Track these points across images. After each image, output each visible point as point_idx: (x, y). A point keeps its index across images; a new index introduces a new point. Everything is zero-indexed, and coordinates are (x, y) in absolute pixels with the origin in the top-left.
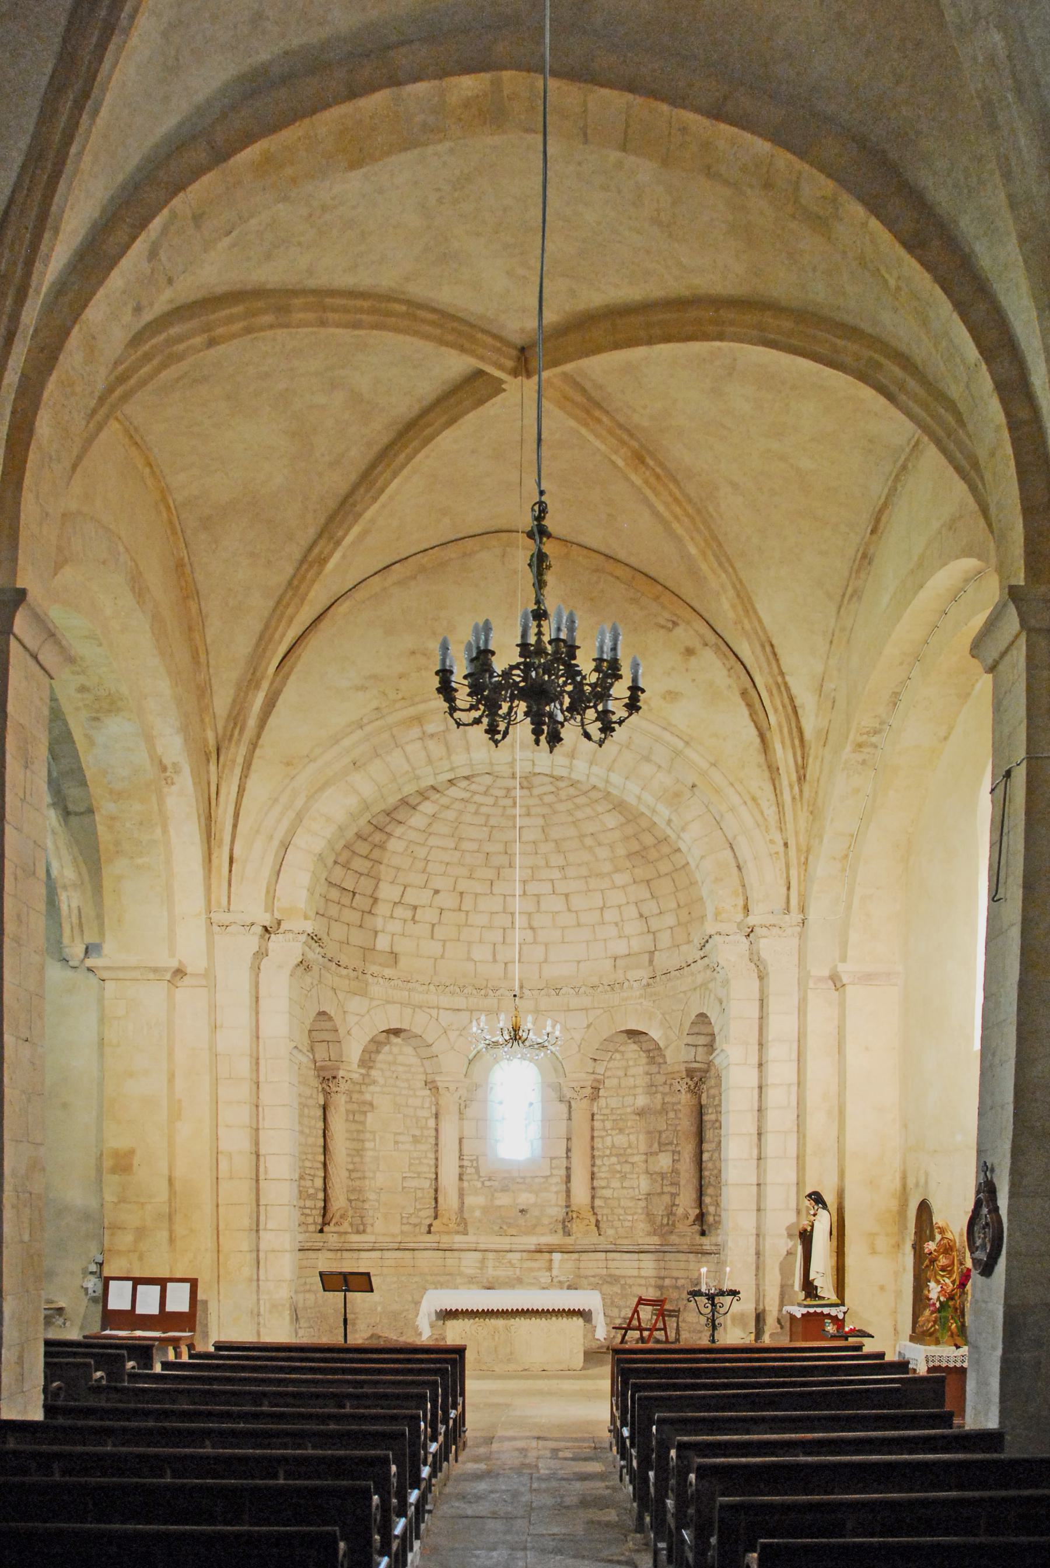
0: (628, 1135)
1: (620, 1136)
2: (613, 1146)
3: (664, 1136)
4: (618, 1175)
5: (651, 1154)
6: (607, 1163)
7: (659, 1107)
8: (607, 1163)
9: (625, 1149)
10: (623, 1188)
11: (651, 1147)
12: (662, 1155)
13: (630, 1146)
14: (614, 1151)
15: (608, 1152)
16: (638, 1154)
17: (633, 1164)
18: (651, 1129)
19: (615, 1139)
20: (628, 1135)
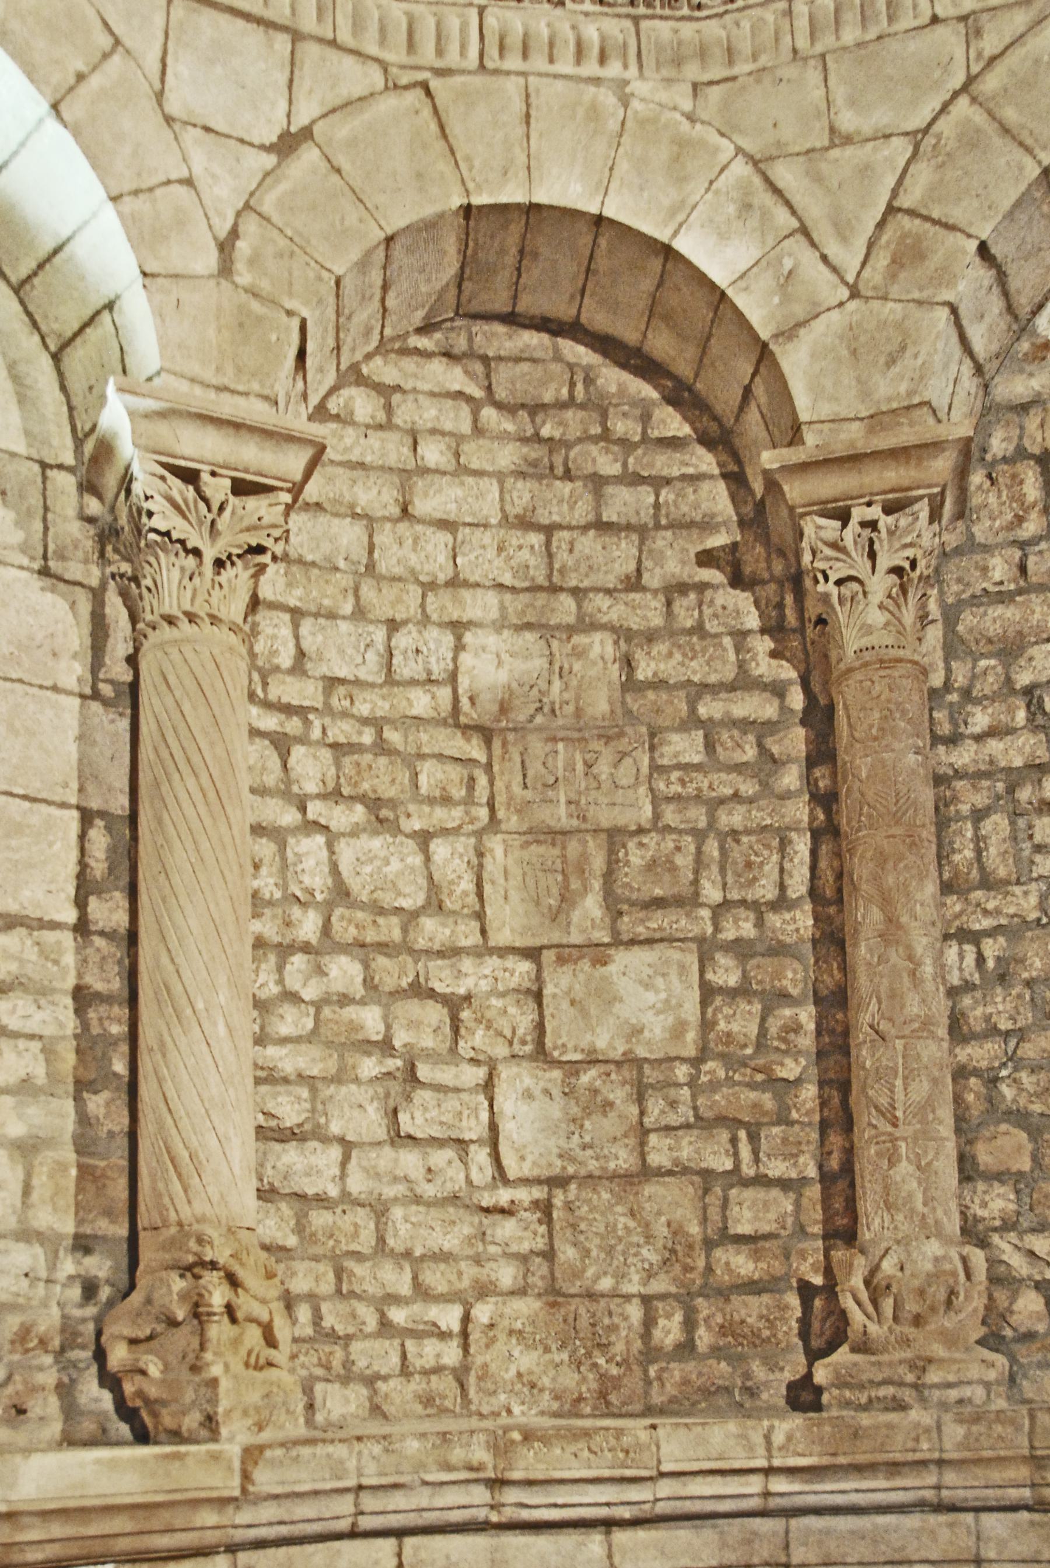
0: (424, 839)
1: (376, 844)
2: (341, 892)
3: (635, 856)
4: (369, 1066)
5: (566, 954)
6: (309, 993)
7: (599, 704)
8: (309, 993)
9: (410, 918)
10: (399, 1138)
11: (557, 916)
12: (639, 958)
13: (435, 904)
14: (344, 930)
15: (308, 927)
16: (485, 950)
17: (454, 1004)
18: (560, 816)
19: (347, 853)
20: (424, 839)
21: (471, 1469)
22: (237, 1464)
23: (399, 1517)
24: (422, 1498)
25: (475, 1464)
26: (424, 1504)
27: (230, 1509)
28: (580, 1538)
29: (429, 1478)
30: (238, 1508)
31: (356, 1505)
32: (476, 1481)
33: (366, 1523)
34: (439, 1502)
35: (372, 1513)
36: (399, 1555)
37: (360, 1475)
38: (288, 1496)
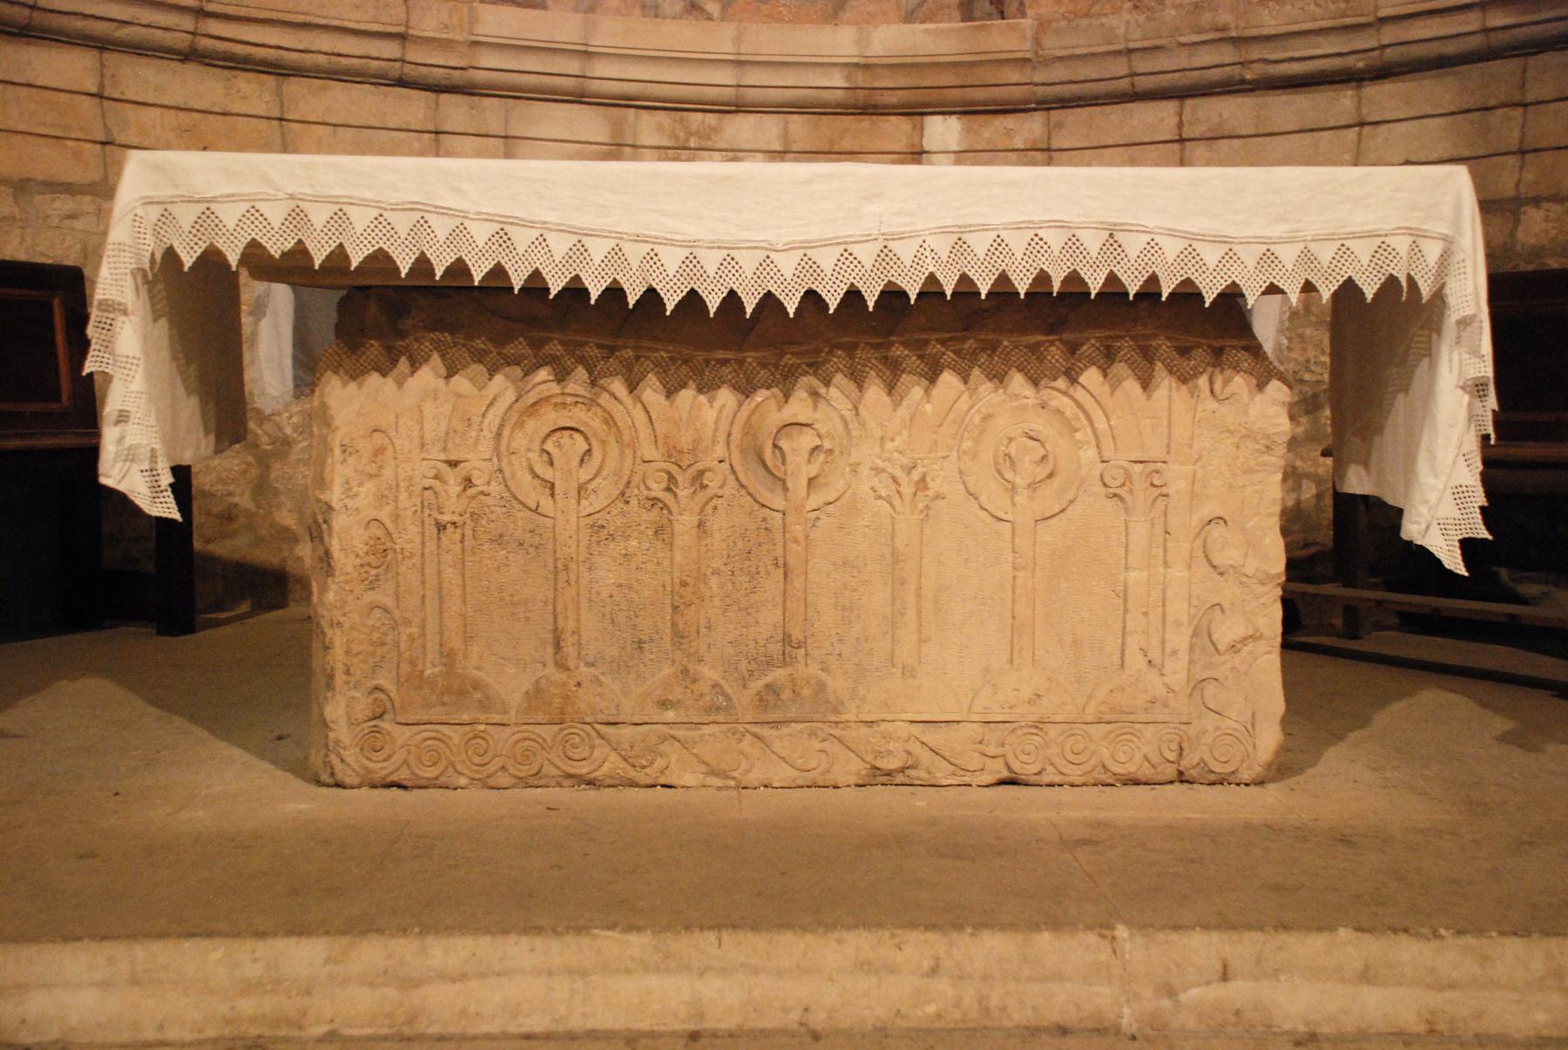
21: (1217, 30)
22: (1029, 33)
23: (1168, 76)
24: (1180, 60)
25: (1220, 25)
26: (1185, 64)
27: (1028, 71)
28: (1334, 94)
29: (1183, 39)
30: (1034, 68)
31: (1130, 66)
32: (1221, 40)
33: (1144, 83)
34: (1197, 62)
35: (1144, 74)
36: (1180, 115)
37: (1127, 40)
38: (1070, 58)
